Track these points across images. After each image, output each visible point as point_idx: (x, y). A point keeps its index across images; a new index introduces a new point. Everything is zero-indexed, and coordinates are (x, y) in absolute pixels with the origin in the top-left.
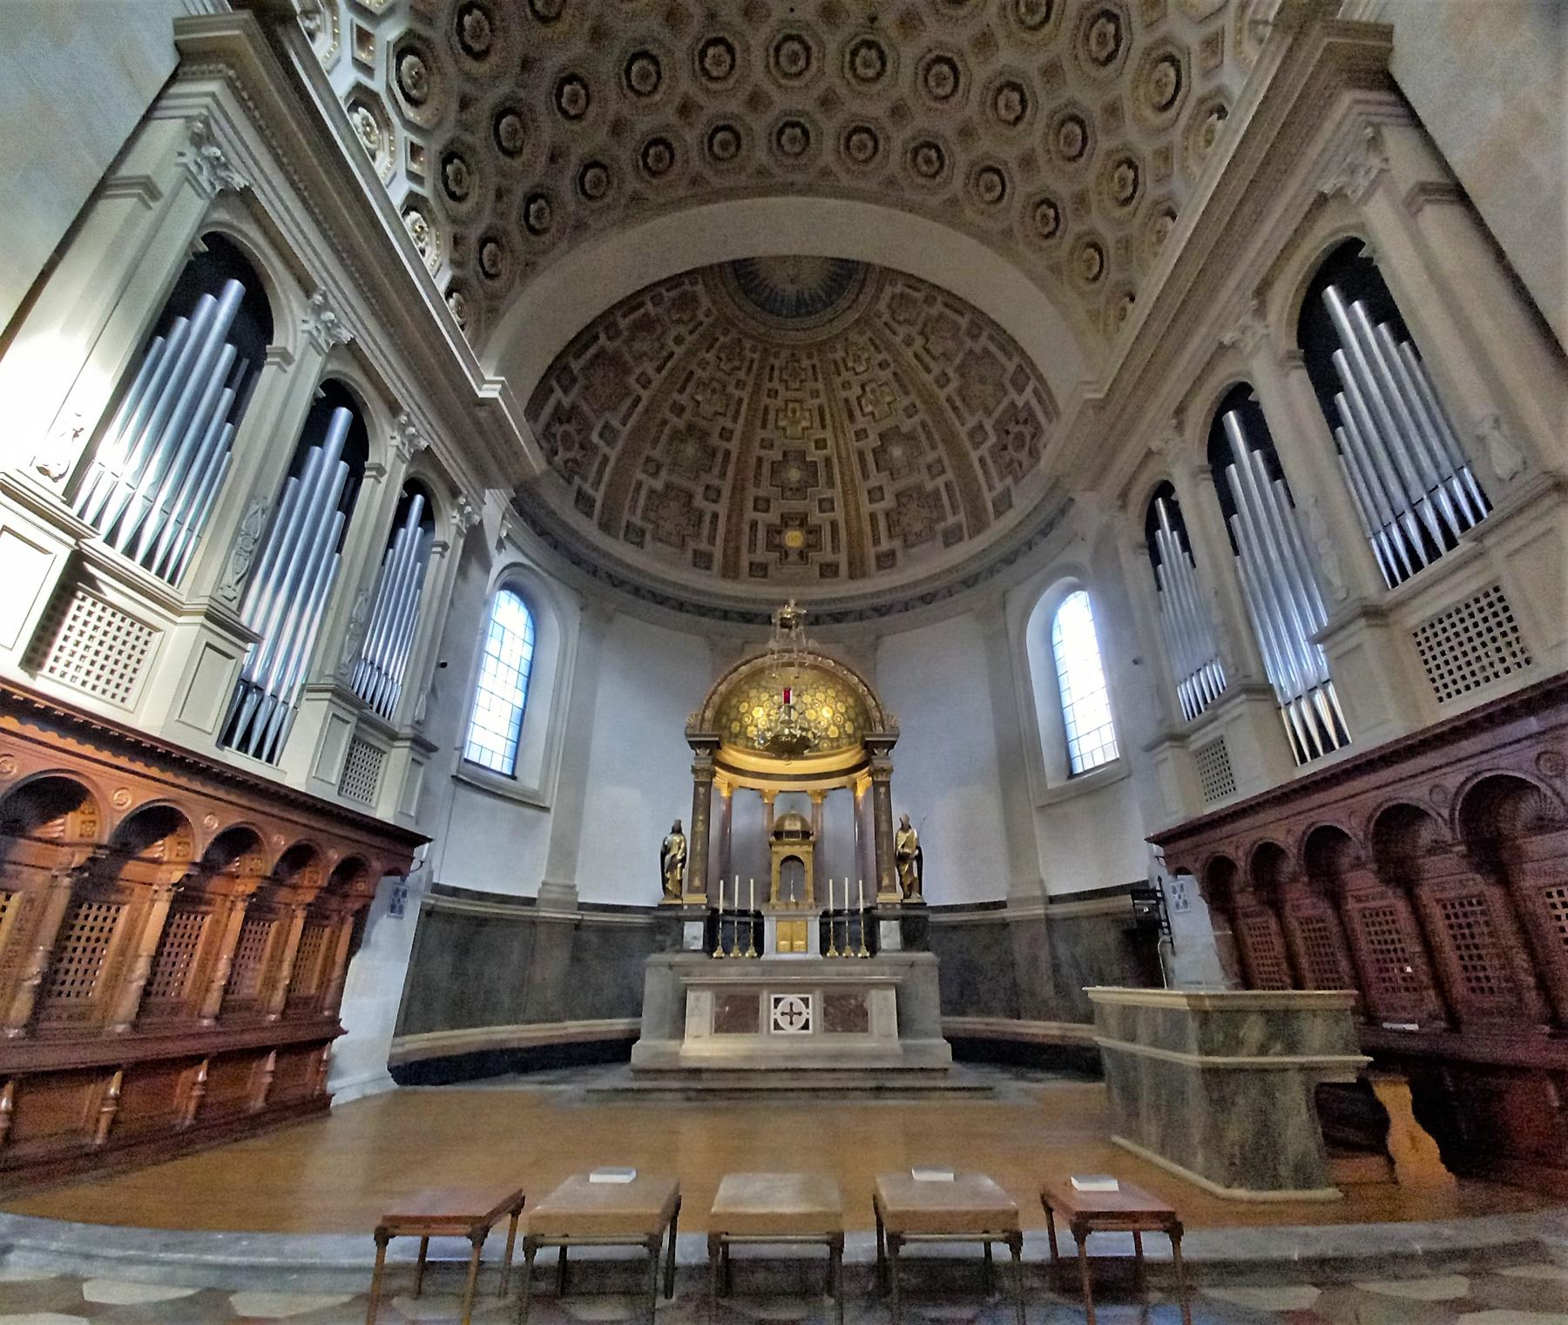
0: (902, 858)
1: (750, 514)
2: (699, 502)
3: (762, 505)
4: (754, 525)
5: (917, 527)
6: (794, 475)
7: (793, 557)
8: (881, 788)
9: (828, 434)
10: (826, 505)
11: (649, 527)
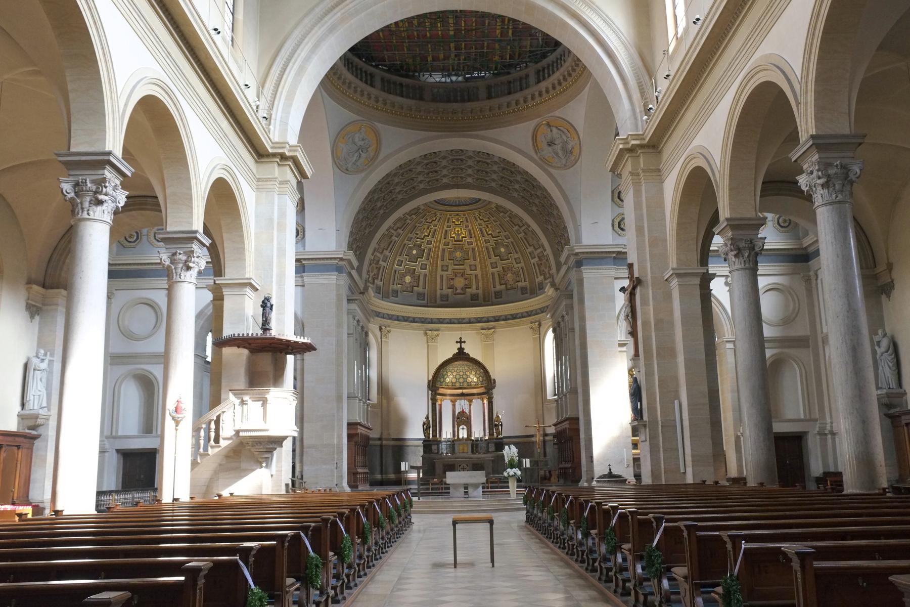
0: (496, 425)
1: (439, 272)
2: (418, 270)
4: (442, 277)
5: (512, 283)
6: (458, 254)
8: (490, 403)
9: (473, 240)
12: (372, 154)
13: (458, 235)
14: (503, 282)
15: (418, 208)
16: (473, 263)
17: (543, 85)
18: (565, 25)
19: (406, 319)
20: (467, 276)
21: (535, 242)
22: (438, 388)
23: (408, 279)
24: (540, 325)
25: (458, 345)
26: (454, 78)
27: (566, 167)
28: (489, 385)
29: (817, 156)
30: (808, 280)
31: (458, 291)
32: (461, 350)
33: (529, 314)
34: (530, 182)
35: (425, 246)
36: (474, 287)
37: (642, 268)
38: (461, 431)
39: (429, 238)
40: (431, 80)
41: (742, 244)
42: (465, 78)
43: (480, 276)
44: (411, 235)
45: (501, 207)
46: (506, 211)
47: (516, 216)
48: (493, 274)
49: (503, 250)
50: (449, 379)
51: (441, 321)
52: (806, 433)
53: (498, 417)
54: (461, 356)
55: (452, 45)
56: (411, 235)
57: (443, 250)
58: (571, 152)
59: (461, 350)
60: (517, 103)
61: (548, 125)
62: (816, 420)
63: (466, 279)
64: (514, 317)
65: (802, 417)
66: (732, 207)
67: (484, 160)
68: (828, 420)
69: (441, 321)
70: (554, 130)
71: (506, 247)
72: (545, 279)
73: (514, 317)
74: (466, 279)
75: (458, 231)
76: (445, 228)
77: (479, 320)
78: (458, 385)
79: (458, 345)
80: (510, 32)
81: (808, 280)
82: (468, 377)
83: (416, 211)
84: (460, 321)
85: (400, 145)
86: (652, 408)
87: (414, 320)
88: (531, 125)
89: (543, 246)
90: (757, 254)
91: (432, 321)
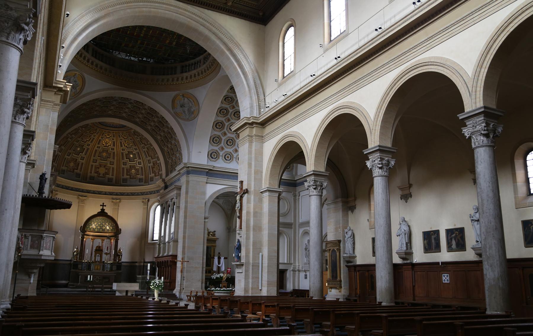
1: (91, 163)
2: (79, 160)
3: (95, 161)
4: (92, 166)
6: (104, 154)
7: (101, 175)
10: (112, 163)
11: (66, 168)
12: (78, 91)
13: (107, 143)
14: (129, 174)
15: (88, 125)
16: (112, 160)
17: (185, 75)
18: (223, 53)
19: (67, 188)
20: (107, 168)
21: (153, 155)
22: (86, 231)
23: (72, 164)
24: (148, 201)
25: (101, 207)
26: (132, 58)
27: (188, 120)
28: (117, 231)
29: (379, 154)
30: (295, 196)
31: (101, 175)
32: (103, 210)
33: (142, 194)
34: (163, 122)
35: (86, 147)
36: (111, 174)
37: (249, 184)
38: (97, 257)
39: (89, 143)
40: (119, 56)
41: (318, 183)
42: (138, 60)
43: (115, 169)
44: (79, 139)
45: (137, 132)
46: (138, 134)
47: (145, 139)
48: (123, 168)
49: (131, 156)
50: (94, 225)
51: (88, 192)
52: (287, 270)
53: (120, 250)
54: (102, 213)
55: (139, 42)
56: (79, 139)
57: (96, 150)
58: (193, 113)
59: (103, 210)
60: (168, 80)
61: (183, 96)
62: (292, 264)
63: (106, 169)
64: (133, 194)
65: (286, 262)
66: (315, 165)
67: (139, 105)
68: (297, 264)
69: (88, 192)
70: (186, 99)
71: (134, 155)
72: (155, 176)
73: (133, 194)
74: (106, 169)
75: (108, 141)
76: (100, 138)
77: (111, 194)
78: (96, 230)
79: (101, 207)
80: (174, 43)
81: (295, 196)
82: (103, 226)
83: (86, 126)
84: (100, 193)
85: (96, 87)
86: (247, 256)
87: (72, 189)
88: (174, 94)
89: (158, 157)
90: (323, 189)
91: (83, 191)
